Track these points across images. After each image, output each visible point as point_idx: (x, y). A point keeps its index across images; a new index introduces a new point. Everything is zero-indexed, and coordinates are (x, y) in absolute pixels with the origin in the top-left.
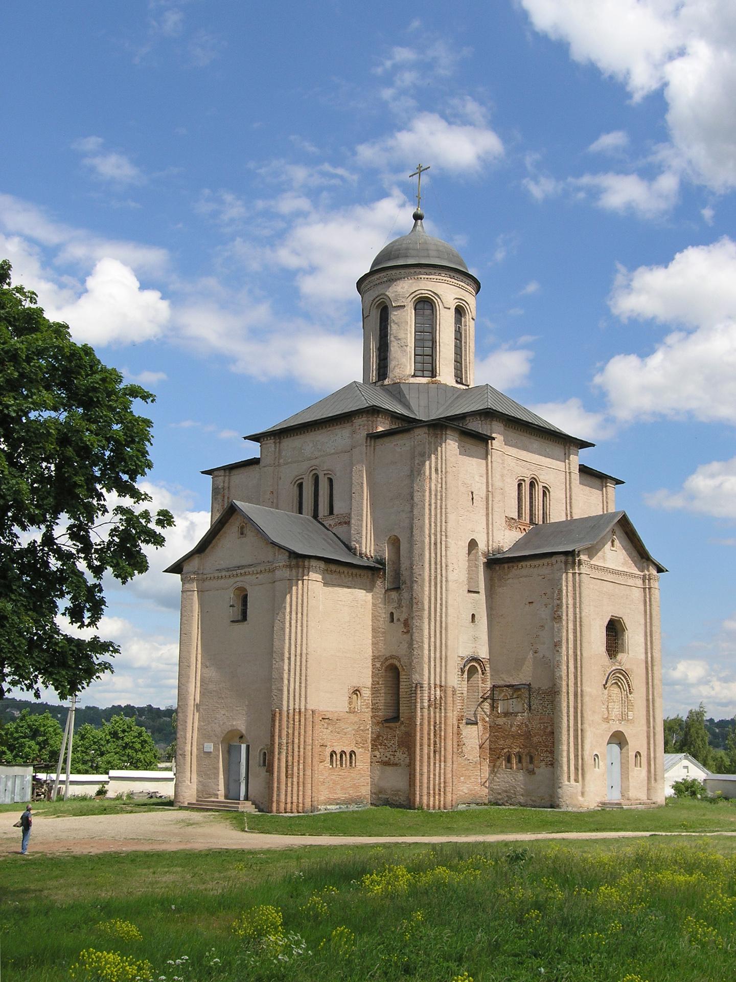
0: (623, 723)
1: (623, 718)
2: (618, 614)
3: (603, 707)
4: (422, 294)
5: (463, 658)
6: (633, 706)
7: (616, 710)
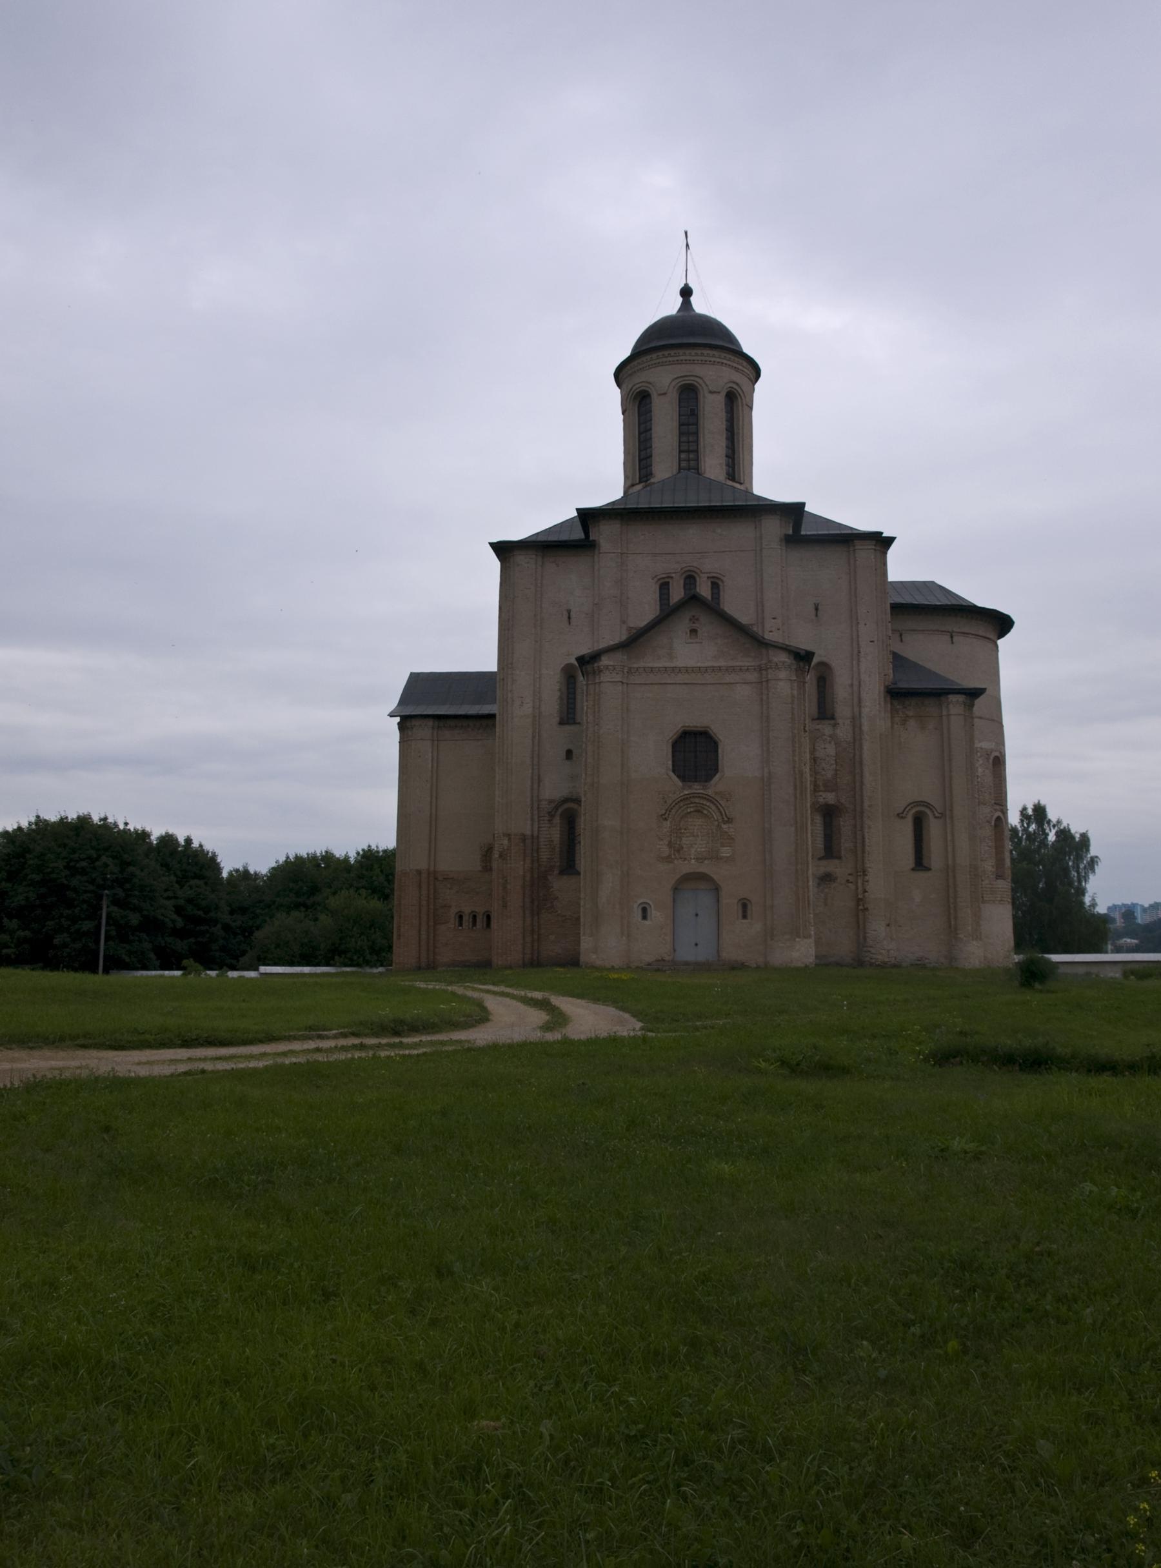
0: (706, 862)
2: (695, 721)
3: (661, 843)
4: (637, 389)
5: (551, 801)
6: (733, 839)
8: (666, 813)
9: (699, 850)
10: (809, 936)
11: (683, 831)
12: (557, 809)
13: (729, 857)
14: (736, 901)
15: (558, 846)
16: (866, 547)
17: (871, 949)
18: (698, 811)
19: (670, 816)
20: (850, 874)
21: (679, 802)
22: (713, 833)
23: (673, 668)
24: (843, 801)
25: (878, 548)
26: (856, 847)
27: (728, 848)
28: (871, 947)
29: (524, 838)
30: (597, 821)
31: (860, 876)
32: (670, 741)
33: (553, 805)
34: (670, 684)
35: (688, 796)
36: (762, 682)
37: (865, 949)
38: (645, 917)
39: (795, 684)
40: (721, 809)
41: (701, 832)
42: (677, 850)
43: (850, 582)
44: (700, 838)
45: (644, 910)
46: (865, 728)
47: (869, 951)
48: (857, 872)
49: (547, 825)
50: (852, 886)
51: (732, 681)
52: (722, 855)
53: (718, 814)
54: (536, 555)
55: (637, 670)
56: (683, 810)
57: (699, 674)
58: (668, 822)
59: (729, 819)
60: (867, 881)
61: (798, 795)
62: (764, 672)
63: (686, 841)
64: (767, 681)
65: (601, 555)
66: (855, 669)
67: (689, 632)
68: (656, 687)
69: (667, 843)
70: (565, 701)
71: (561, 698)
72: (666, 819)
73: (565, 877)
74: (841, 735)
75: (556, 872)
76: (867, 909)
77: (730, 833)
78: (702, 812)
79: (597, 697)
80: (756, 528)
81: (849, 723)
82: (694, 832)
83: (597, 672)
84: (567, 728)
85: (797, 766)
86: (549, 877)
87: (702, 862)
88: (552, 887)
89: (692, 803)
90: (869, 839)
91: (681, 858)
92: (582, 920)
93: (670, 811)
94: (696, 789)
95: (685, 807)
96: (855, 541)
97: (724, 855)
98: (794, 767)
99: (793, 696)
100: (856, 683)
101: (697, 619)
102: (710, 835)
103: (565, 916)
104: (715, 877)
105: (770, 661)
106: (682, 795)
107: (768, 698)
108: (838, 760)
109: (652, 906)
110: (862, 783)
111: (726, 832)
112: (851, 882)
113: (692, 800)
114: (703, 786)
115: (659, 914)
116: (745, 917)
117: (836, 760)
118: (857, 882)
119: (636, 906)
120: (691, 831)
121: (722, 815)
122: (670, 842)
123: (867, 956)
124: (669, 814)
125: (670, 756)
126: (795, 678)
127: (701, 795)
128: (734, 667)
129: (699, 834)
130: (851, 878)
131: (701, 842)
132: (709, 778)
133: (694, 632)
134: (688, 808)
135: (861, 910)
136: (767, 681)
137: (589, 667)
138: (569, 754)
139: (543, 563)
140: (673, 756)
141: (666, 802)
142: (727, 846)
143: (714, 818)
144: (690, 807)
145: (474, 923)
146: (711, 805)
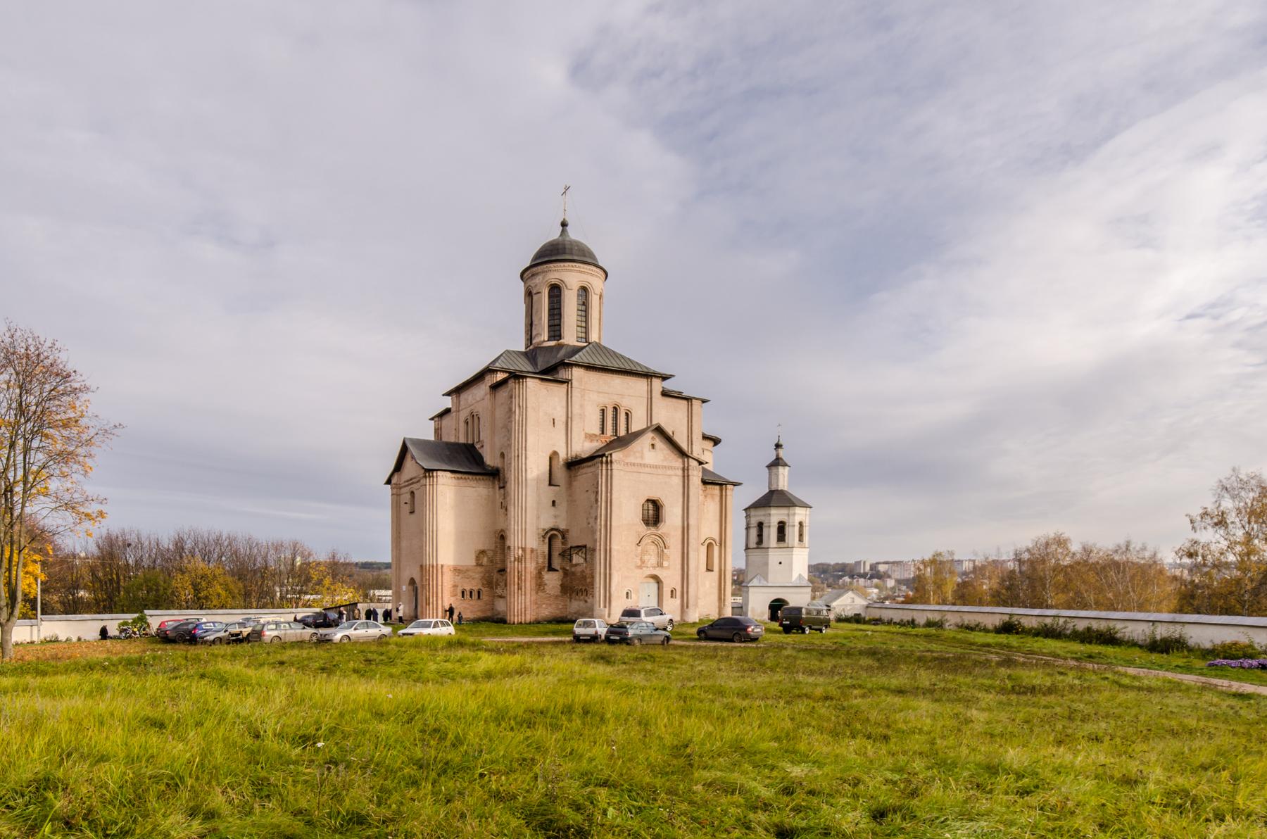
1: (660, 565)
5: (544, 530)
7: (652, 559)
23: (644, 465)
29: (532, 551)
38: (627, 597)
42: (643, 562)
75: (546, 569)
116: (672, 597)
133: (653, 445)
138: (554, 502)
145: (471, 596)
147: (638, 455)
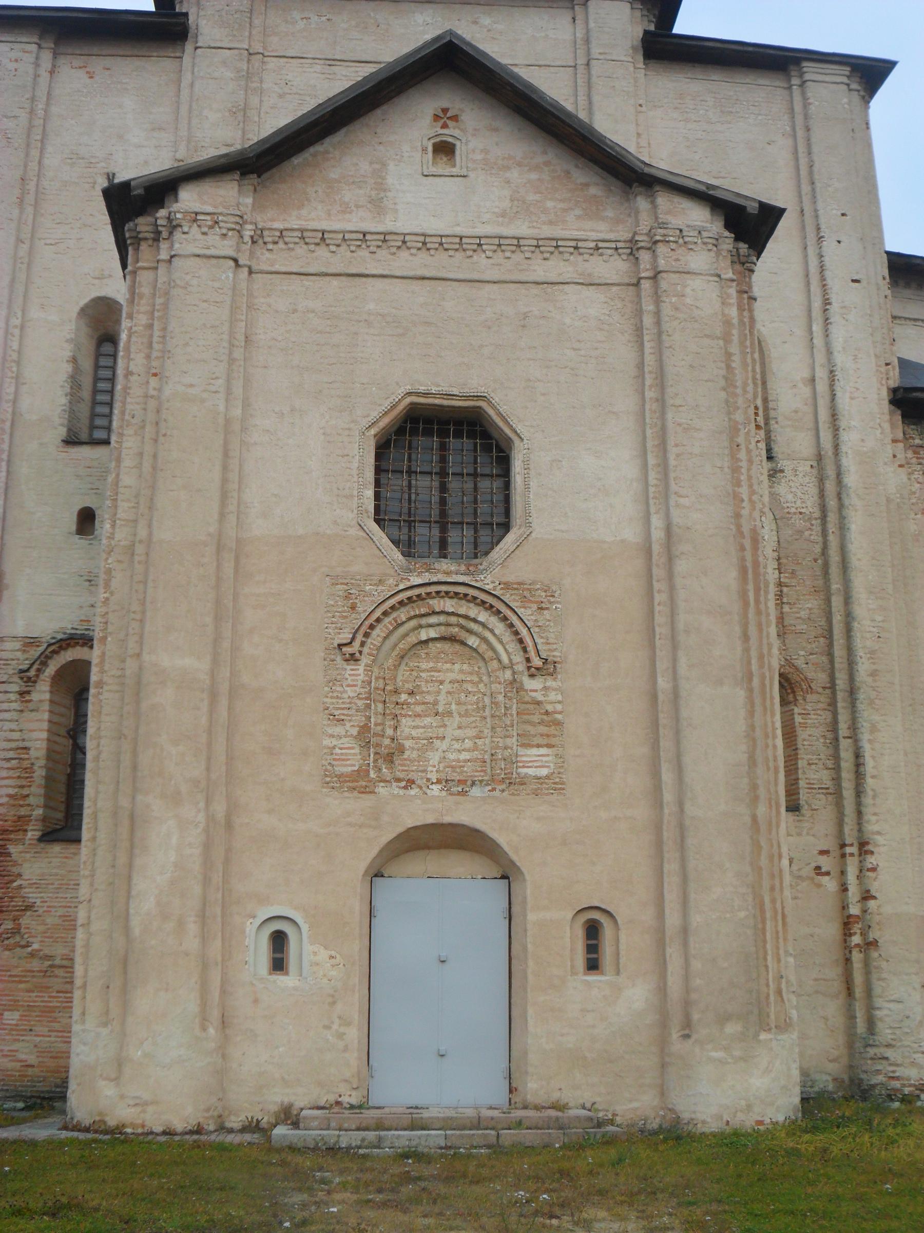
0: (476, 792)
3: (339, 730)
5: (30, 642)
6: (558, 723)
8: (353, 639)
9: (452, 756)
10: (784, 1026)
11: (404, 697)
12: (44, 664)
13: (547, 777)
14: (570, 915)
15: (42, 762)
16: (827, 78)
17: (889, 1053)
18: (452, 639)
19: (366, 650)
20: (823, 853)
21: (393, 608)
22: (496, 704)
23: (385, 237)
24: (800, 663)
25: (854, 86)
26: (837, 780)
27: (543, 751)
28: (888, 1046)
30: (138, 655)
31: (852, 855)
32: (373, 432)
33: (35, 653)
34: (374, 276)
35: (422, 591)
36: (637, 284)
37: (872, 1051)
38: (278, 965)
39: (733, 291)
40: (524, 632)
41: (459, 703)
43: (796, 152)
44: (457, 719)
45: (279, 940)
46: (852, 479)
47: (887, 1059)
48: (843, 846)
49: (15, 705)
50: (830, 884)
51: (552, 277)
52: (523, 771)
53: (513, 646)
54: (40, 47)
55: (281, 236)
56: (406, 635)
57: (459, 255)
58: (361, 668)
59: (546, 661)
60: (874, 869)
61: (751, 595)
62: (645, 256)
63: (414, 727)
64: (654, 278)
65: (199, 51)
66: (818, 341)
67: (430, 149)
68: (335, 282)
69: (354, 731)
70: (86, 394)
71: (74, 381)
72: (352, 659)
73: (57, 848)
74: (790, 497)
75: (32, 834)
76: (874, 944)
77: (550, 708)
78: (463, 643)
79: (159, 301)
80: (574, 19)
81: (808, 469)
82: (436, 703)
83: (165, 234)
84: (85, 452)
85: (745, 512)
86: (12, 849)
87: (463, 793)
88: (20, 875)
89: (434, 613)
90: (873, 757)
91: (398, 780)
92: (79, 970)
93: (366, 635)
94: (448, 573)
95: (413, 623)
96: (805, 64)
97: (531, 771)
98: (738, 516)
99: (727, 323)
100: (821, 374)
101: (455, 118)
102: (487, 713)
103: (48, 957)
104: (502, 839)
105: (663, 225)
106: (401, 587)
107: (658, 323)
108: (783, 561)
109: (305, 928)
110: (849, 618)
111: (538, 703)
112: (828, 874)
113: (437, 604)
114: (468, 566)
115: (323, 954)
116: (593, 965)
117: (779, 559)
118: (843, 873)
119: (251, 927)
120: (430, 698)
121: (525, 650)
122: (365, 729)
123: (878, 1072)
124: (363, 644)
125: (370, 475)
126: (730, 275)
127: (461, 590)
128: (557, 240)
129: (454, 707)
130: (826, 863)
131: (458, 733)
132: (479, 550)
133: (444, 149)
134: (421, 626)
135: (857, 945)
136: (654, 278)
137: (143, 224)
139: (54, 66)
140: (377, 484)
141: (353, 607)
142: (538, 746)
143: (500, 661)
144: (431, 626)
146: (493, 621)
147: (348, 195)
